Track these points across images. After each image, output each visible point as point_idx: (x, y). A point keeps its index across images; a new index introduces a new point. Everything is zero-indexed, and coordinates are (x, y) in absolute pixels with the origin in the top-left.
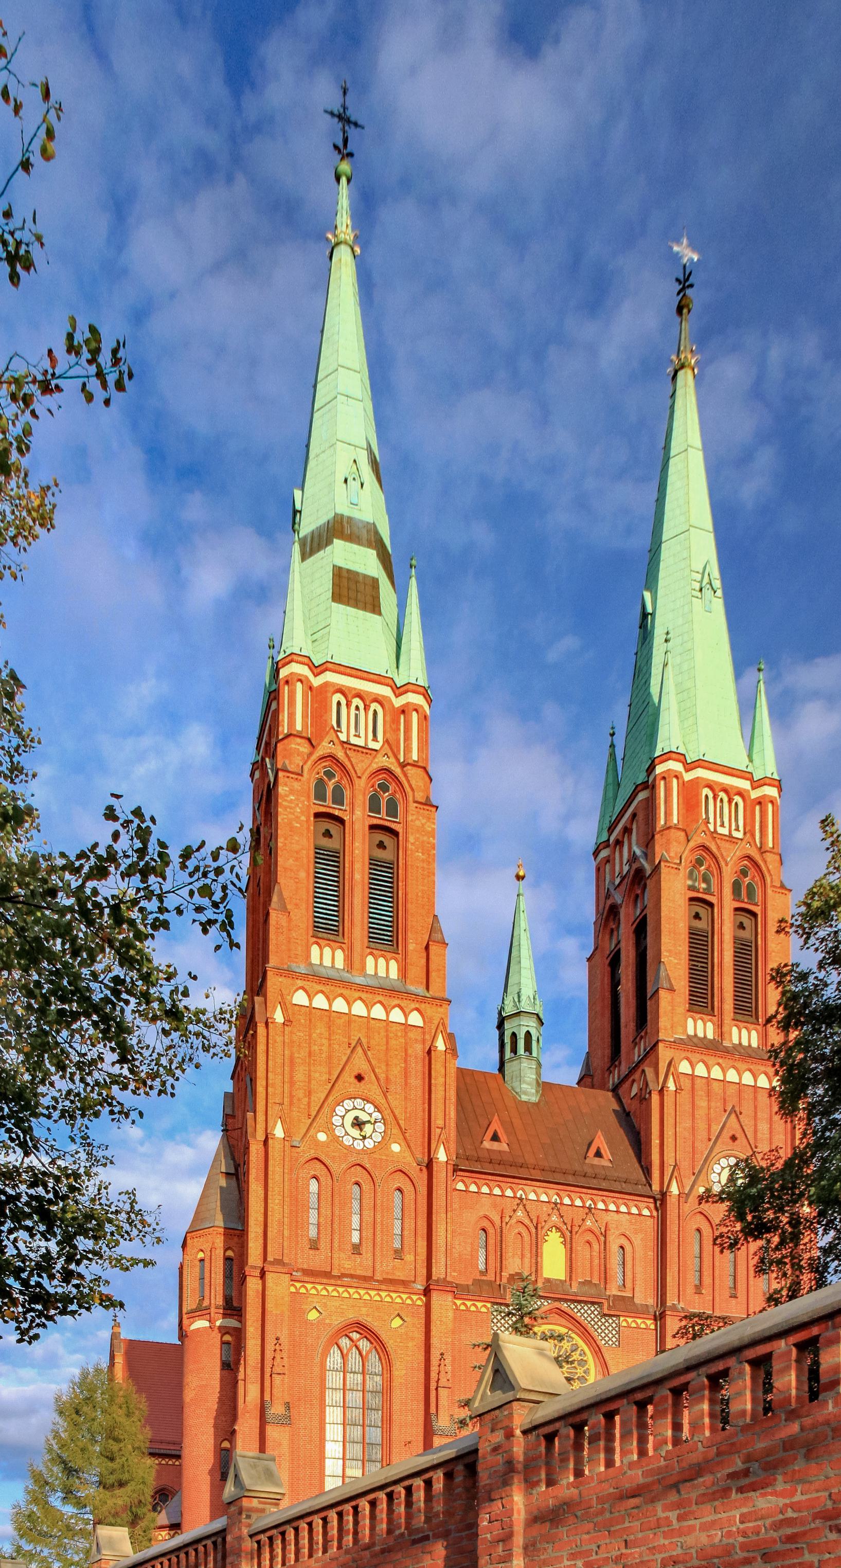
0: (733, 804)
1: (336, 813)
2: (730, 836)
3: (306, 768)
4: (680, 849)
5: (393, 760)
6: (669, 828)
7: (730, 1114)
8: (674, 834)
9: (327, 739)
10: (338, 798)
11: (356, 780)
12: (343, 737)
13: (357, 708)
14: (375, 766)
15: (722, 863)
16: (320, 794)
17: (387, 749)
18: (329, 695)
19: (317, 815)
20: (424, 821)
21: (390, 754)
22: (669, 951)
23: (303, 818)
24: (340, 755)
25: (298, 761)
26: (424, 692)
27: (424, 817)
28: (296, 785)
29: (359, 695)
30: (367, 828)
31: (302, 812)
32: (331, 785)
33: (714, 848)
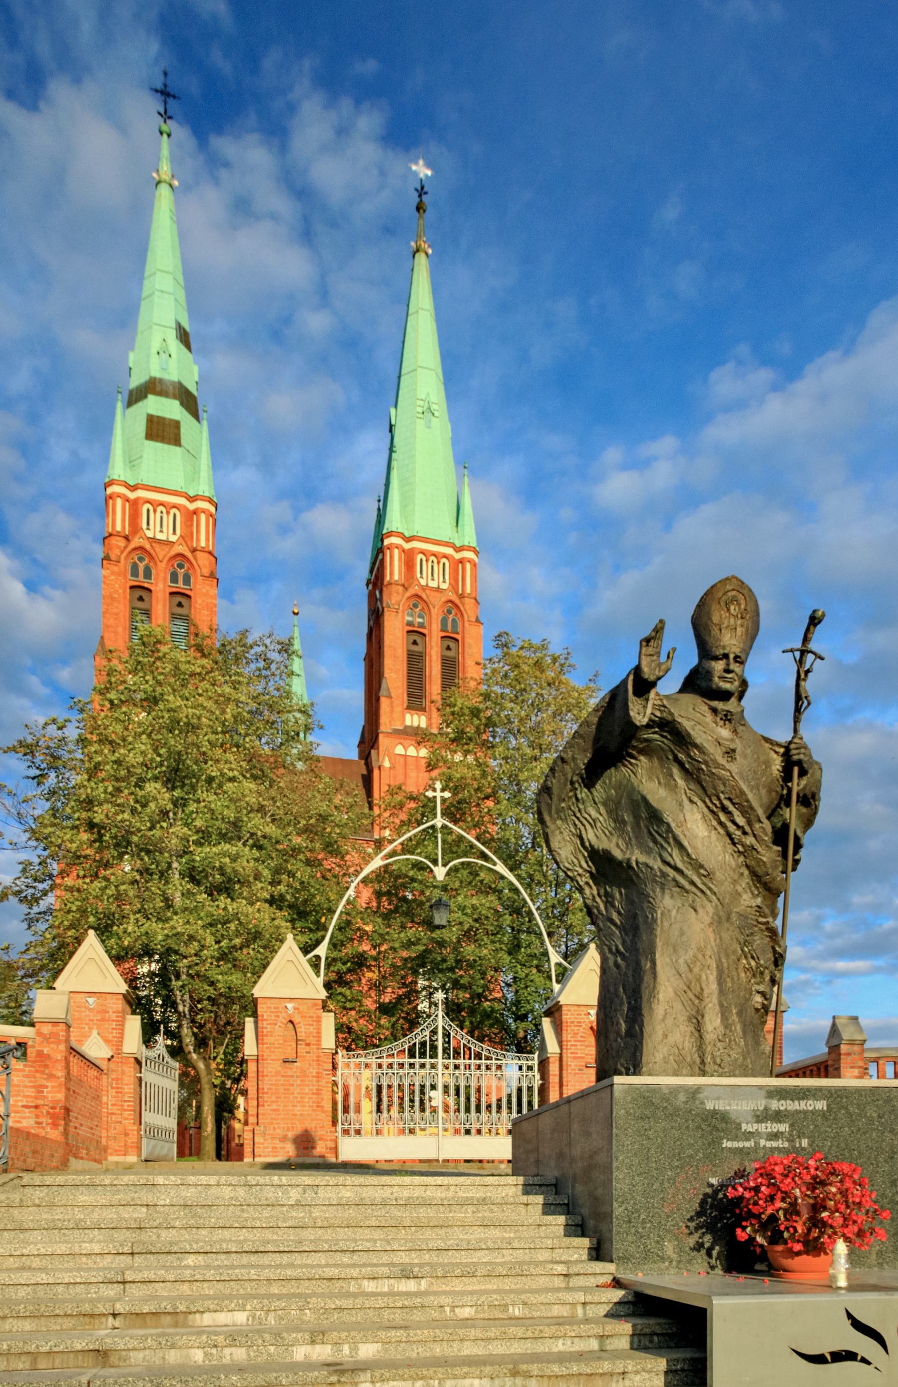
0: (441, 565)
1: (146, 585)
2: (438, 587)
3: (123, 557)
4: (399, 598)
6: (390, 584)
8: (394, 588)
9: (138, 536)
10: (148, 574)
11: (159, 563)
12: (149, 534)
13: (162, 512)
14: (172, 553)
15: (431, 607)
16: (135, 573)
17: (181, 541)
18: (140, 506)
19: (132, 587)
20: (208, 588)
21: (184, 544)
22: (390, 669)
23: (121, 591)
24: (147, 546)
25: (117, 552)
26: (210, 501)
27: (208, 585)
28: (116, 569)
29: (162, 504)
30: (167, 595)
31: (120, 587)
32: (141, 566)
33: (424, 596)
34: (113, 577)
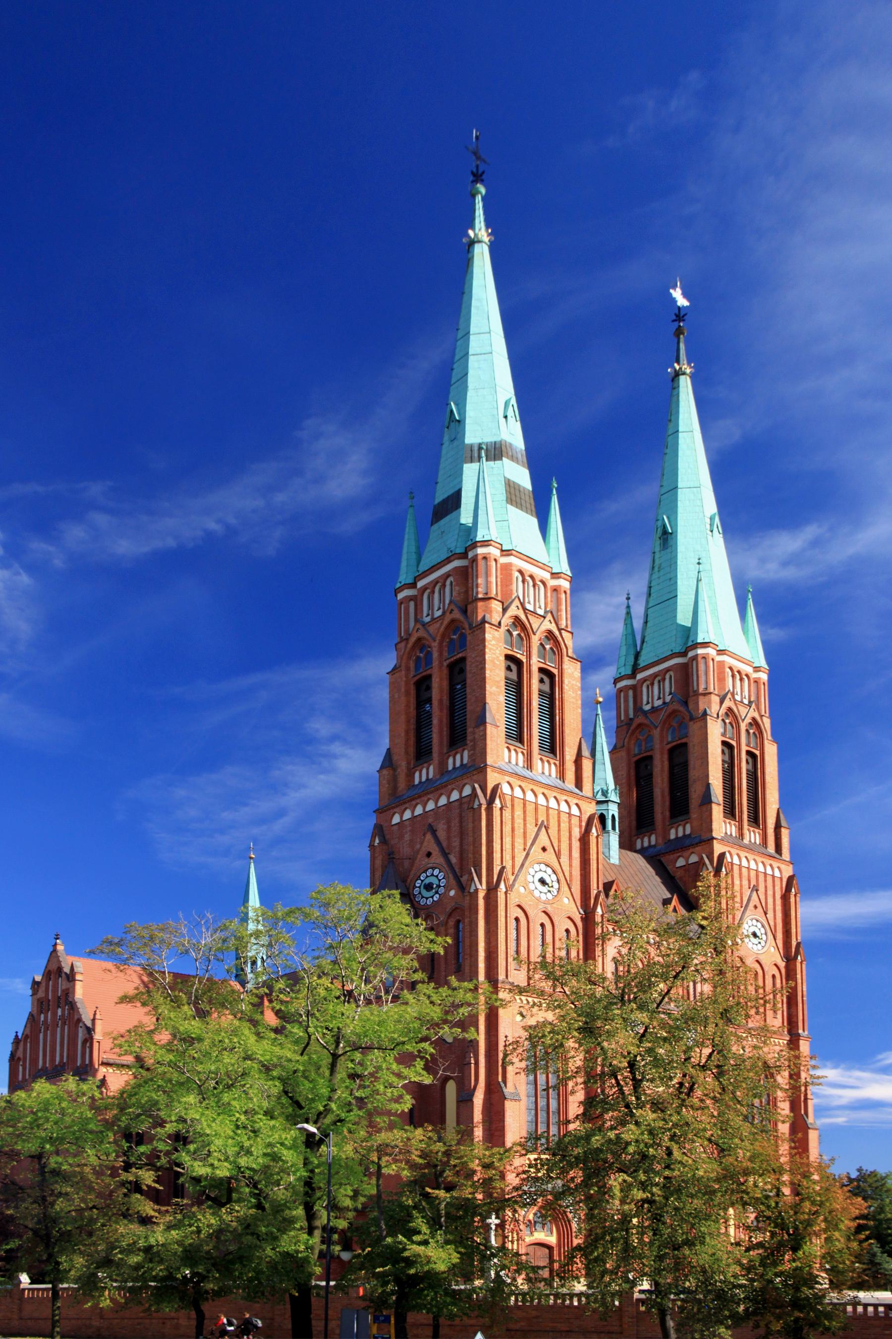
5: (554, 624)
7: (752, 891)
28: (496, 633)
34: (493, 642)
